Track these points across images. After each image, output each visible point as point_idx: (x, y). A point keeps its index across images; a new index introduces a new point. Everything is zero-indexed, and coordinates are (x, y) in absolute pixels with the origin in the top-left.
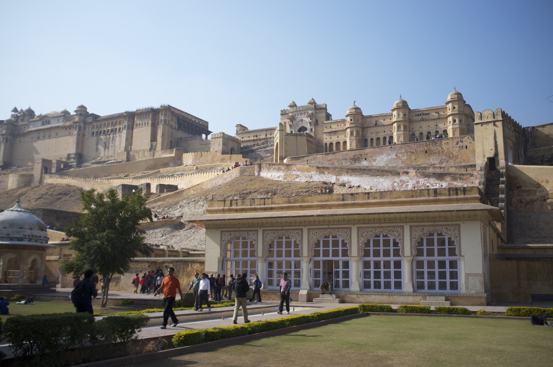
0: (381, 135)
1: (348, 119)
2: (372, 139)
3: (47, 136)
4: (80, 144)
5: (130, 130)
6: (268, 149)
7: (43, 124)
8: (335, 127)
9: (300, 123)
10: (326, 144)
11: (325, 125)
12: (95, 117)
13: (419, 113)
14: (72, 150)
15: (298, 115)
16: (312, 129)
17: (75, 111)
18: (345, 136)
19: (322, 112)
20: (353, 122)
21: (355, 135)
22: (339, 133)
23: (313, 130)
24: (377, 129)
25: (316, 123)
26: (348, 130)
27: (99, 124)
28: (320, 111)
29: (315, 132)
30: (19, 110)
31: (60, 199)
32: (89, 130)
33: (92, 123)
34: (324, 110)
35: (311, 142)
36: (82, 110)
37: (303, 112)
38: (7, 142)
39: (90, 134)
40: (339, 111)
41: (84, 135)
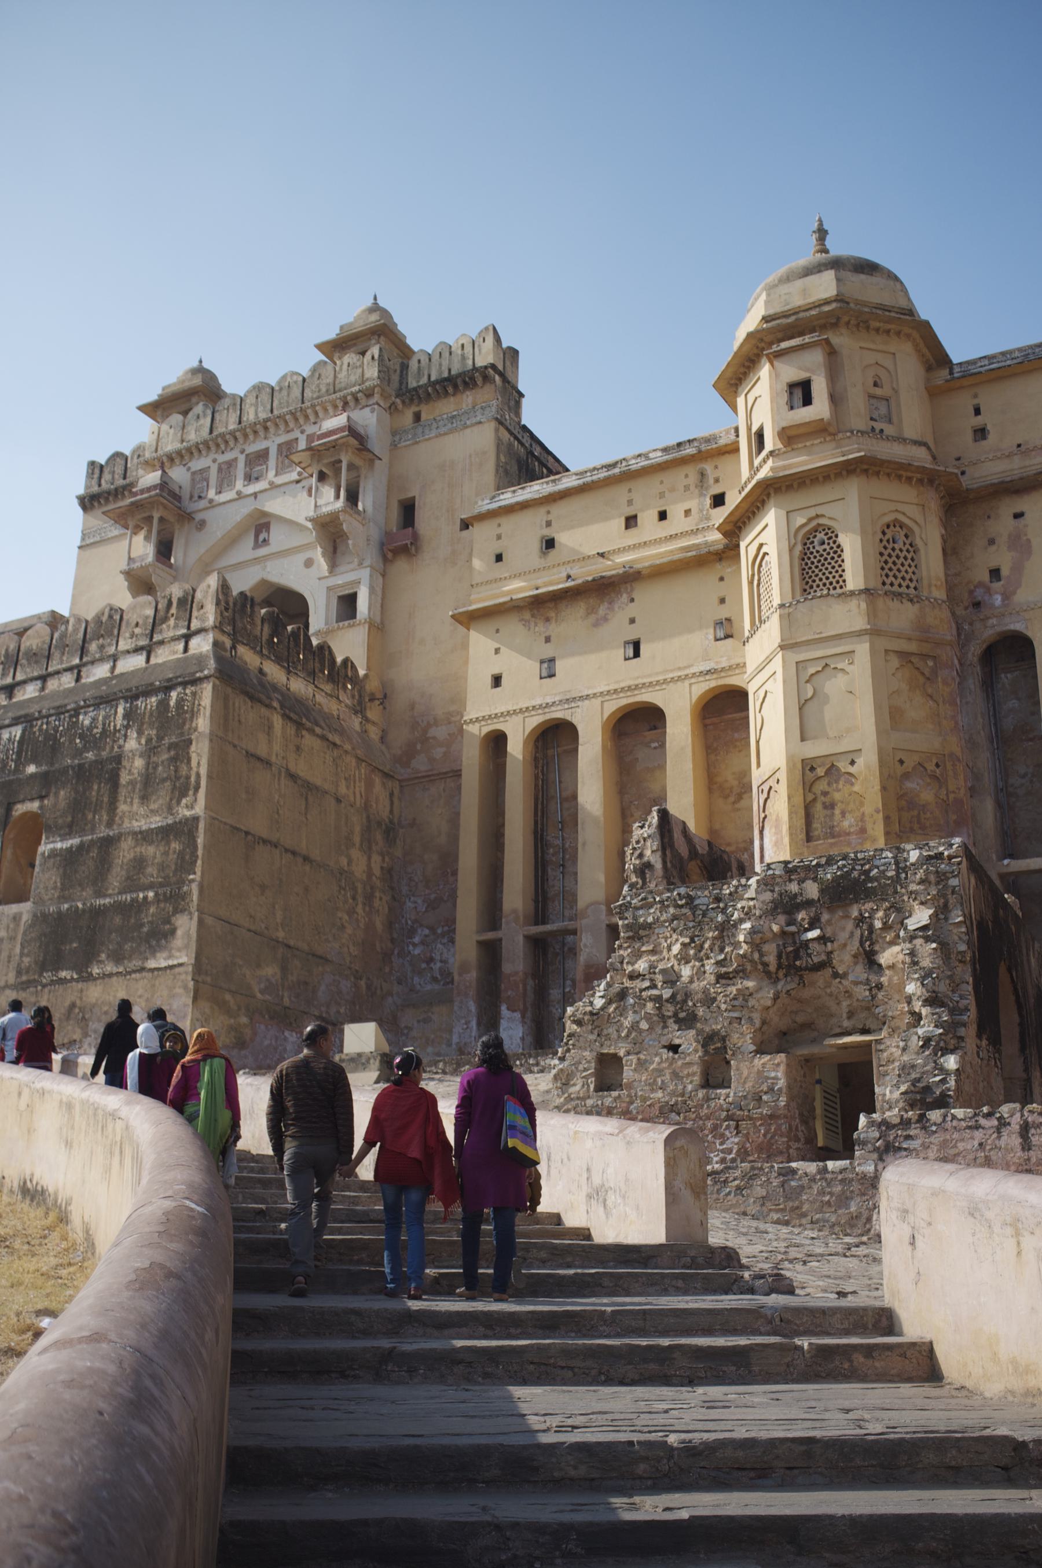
1: (762, 402)
8: (594, 540)
9: (245, 550)
10: (497, 741)
11: (481, 533)
15: (226, 471)
16: (348, 604)
18: (726, 630)
19: (457, 423)
20: (820, 408)
21: (854, 577)
22: (647, 600)
25: (402, 537)
26: (769, 535)
28: (446, 407)
29: (379, 629)
34: (487, 397)
35: (298, 713)
40: (634, 363)
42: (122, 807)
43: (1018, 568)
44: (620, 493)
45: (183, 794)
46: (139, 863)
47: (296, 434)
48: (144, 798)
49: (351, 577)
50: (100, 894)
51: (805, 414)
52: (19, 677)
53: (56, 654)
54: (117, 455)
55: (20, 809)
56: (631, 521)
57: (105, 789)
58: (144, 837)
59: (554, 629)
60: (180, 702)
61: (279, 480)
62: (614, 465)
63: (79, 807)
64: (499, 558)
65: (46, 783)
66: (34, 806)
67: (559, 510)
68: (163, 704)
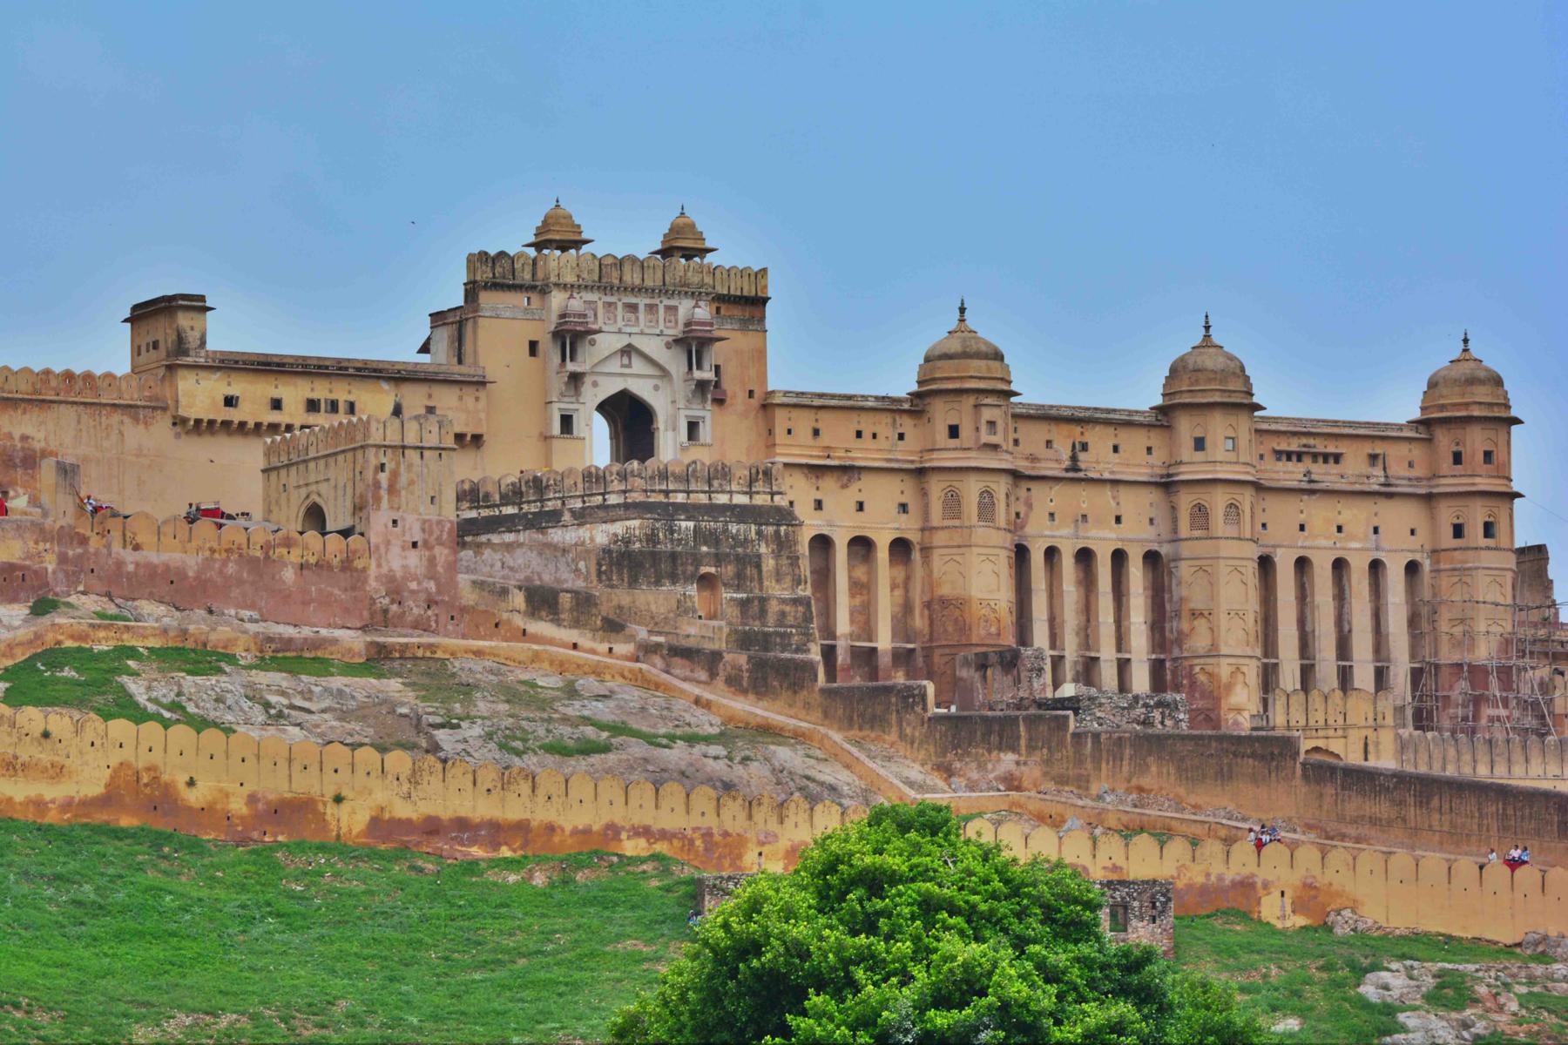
0: (1104, 543)
2: (1051, 553)
6: (556, 535)
9: (614, 366)
13: (1294, 445)
22: (867, 481)
23: (705, 432)
24: (1085, 498)
37: (642, 301)
42: (766, 583)
43: (1027, 515)
44: (854, 416)
45: (799, 583)
46: (783, 614)
47: (657, 301)
48: (778, 581)
49: (701, 413)
50: (764, 625)
51: (993, 439)
52: (671, 487)
53: (692, 480)
54: (502, 254)
55: (704, 570)
56: (859, 434)
57: (755, 571)
58: (783, 601)
59: (821, 483)
60: (787, 534)
61: (647, 331)
62: (850, 397)
63: (740, 576)
64: (789, 432)
65: (718, 559)
66: (713, 570)
67: (822, 415)
68: (777, 532)
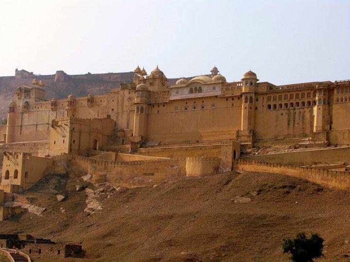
3: (199, 107)
4: (252, 118)
5: (327, 106)
7: (191, 92)
12: (270, 87)
14: (243, 126)
17: (243, 80)
27: (277, 95)
30: (141, 69)
31: (288, 192)
32: (262, 102)
33: (266, 94)
36: (251, 77)
38: (142, 112)
39: (266, 107)
41: (256, 108)
